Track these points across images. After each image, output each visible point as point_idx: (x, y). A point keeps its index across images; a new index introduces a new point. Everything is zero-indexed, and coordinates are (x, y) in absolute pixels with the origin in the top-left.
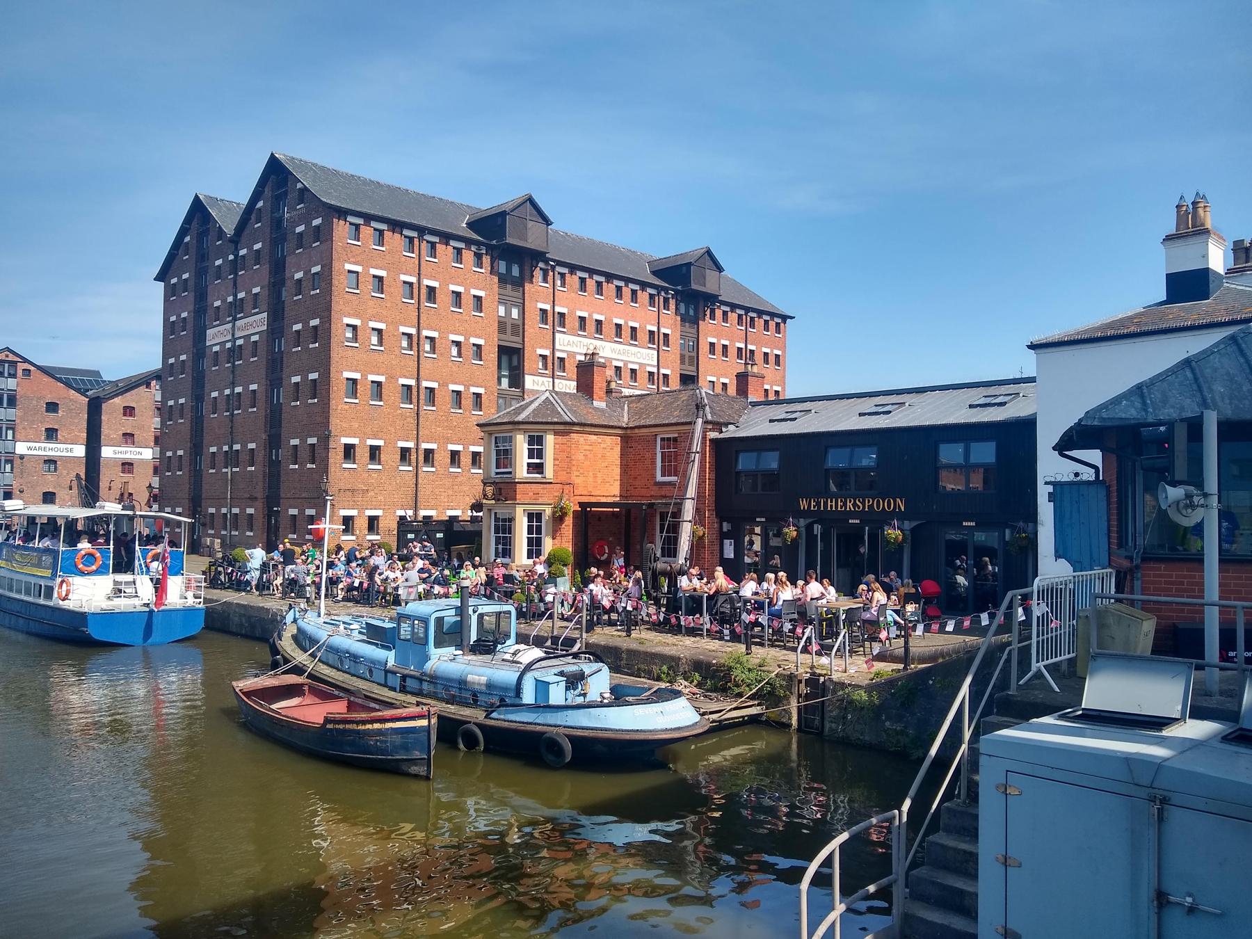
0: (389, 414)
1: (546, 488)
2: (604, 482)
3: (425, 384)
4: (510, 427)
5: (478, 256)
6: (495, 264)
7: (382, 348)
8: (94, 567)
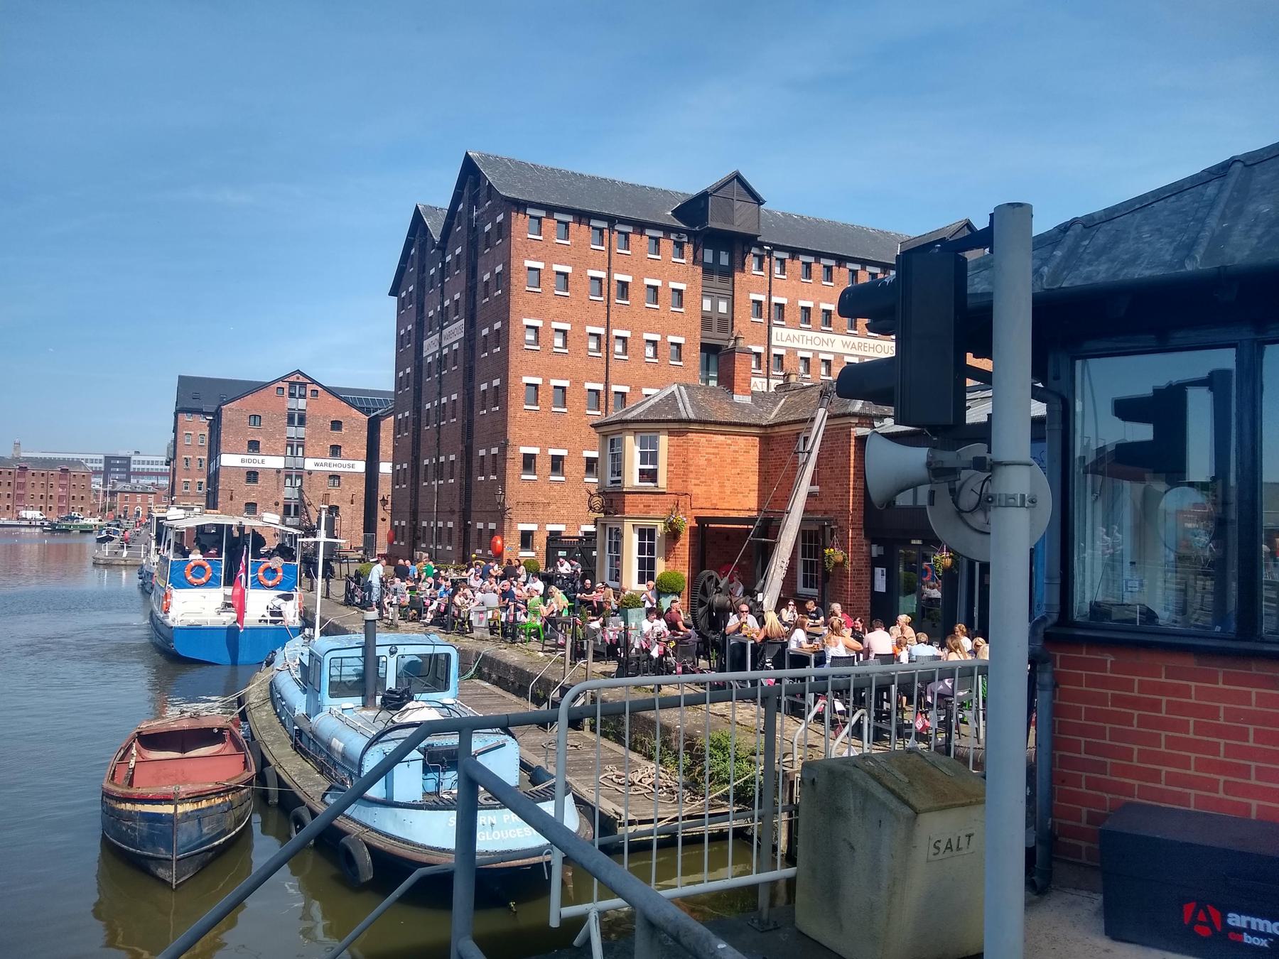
0: (573, 421)
1: (658, 500)
2: (735, 492)
3: (615, 388)
4: (618, 427)
5: (679, 245)
6: (699, 253)
7: (566, 351)
8: (204, 580)
